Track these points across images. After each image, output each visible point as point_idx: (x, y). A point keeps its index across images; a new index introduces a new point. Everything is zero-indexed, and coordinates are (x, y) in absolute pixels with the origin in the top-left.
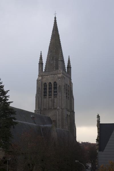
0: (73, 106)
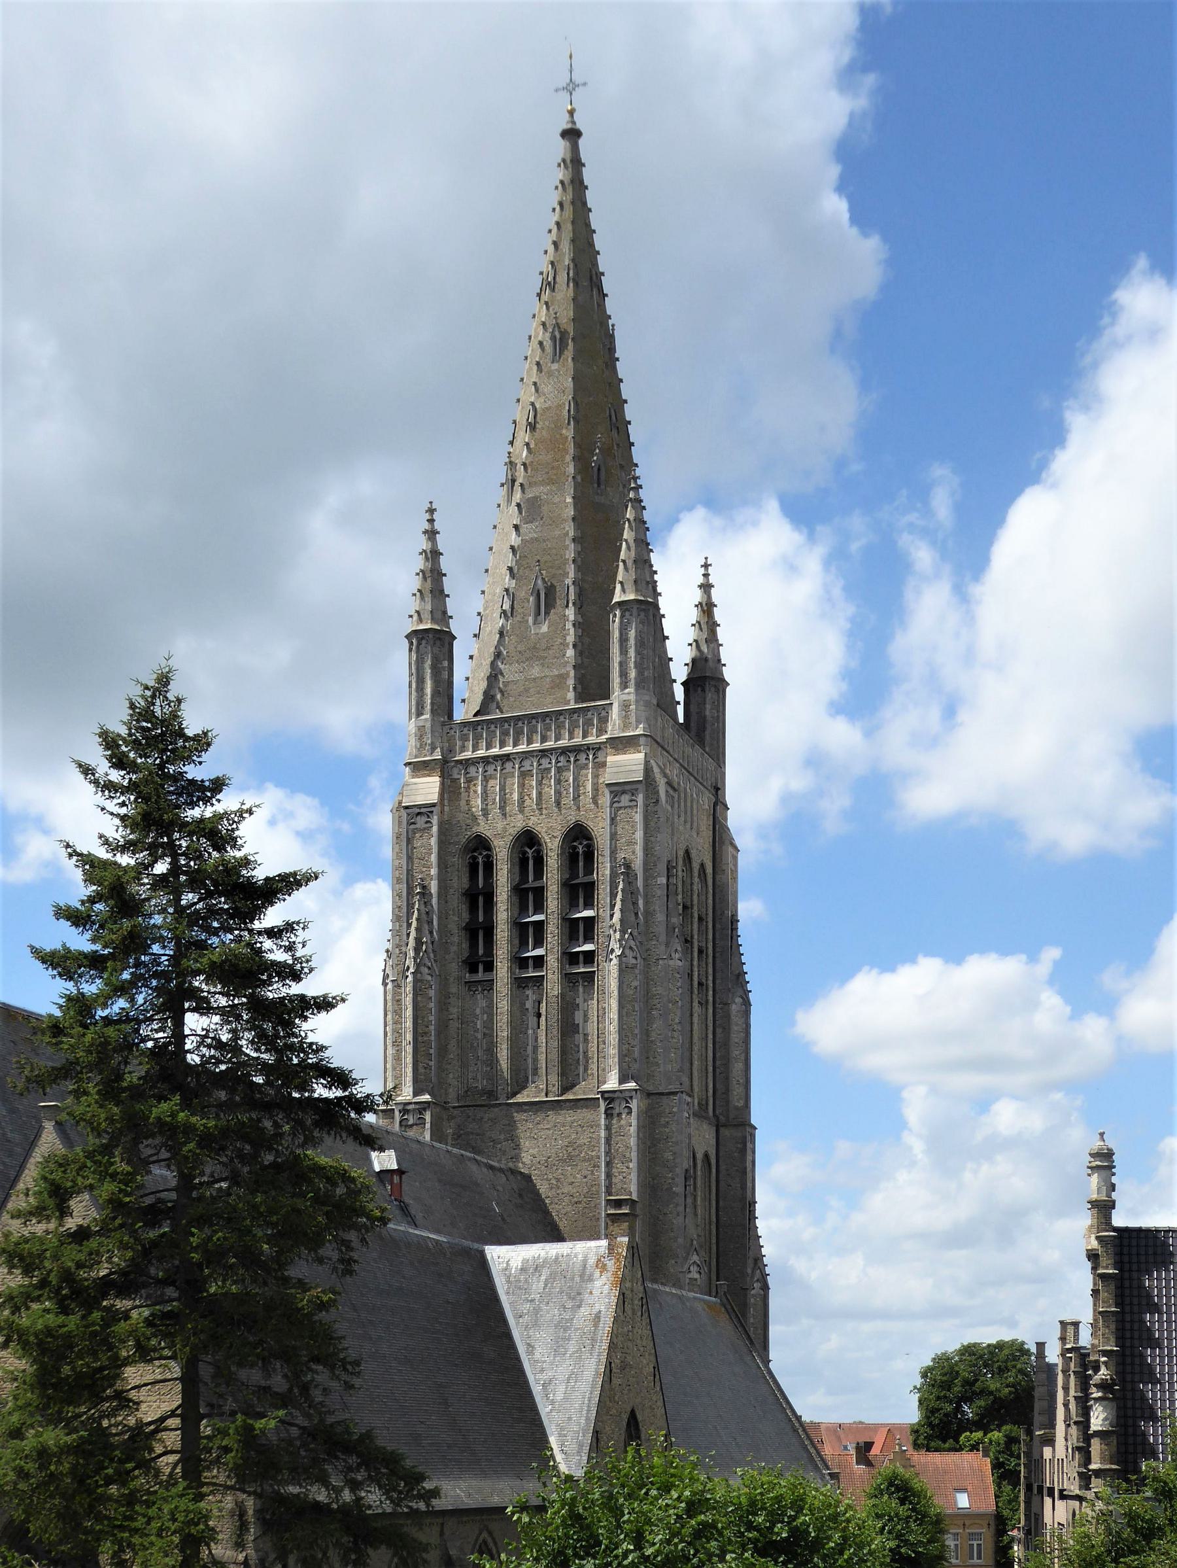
0: (738, 1067)
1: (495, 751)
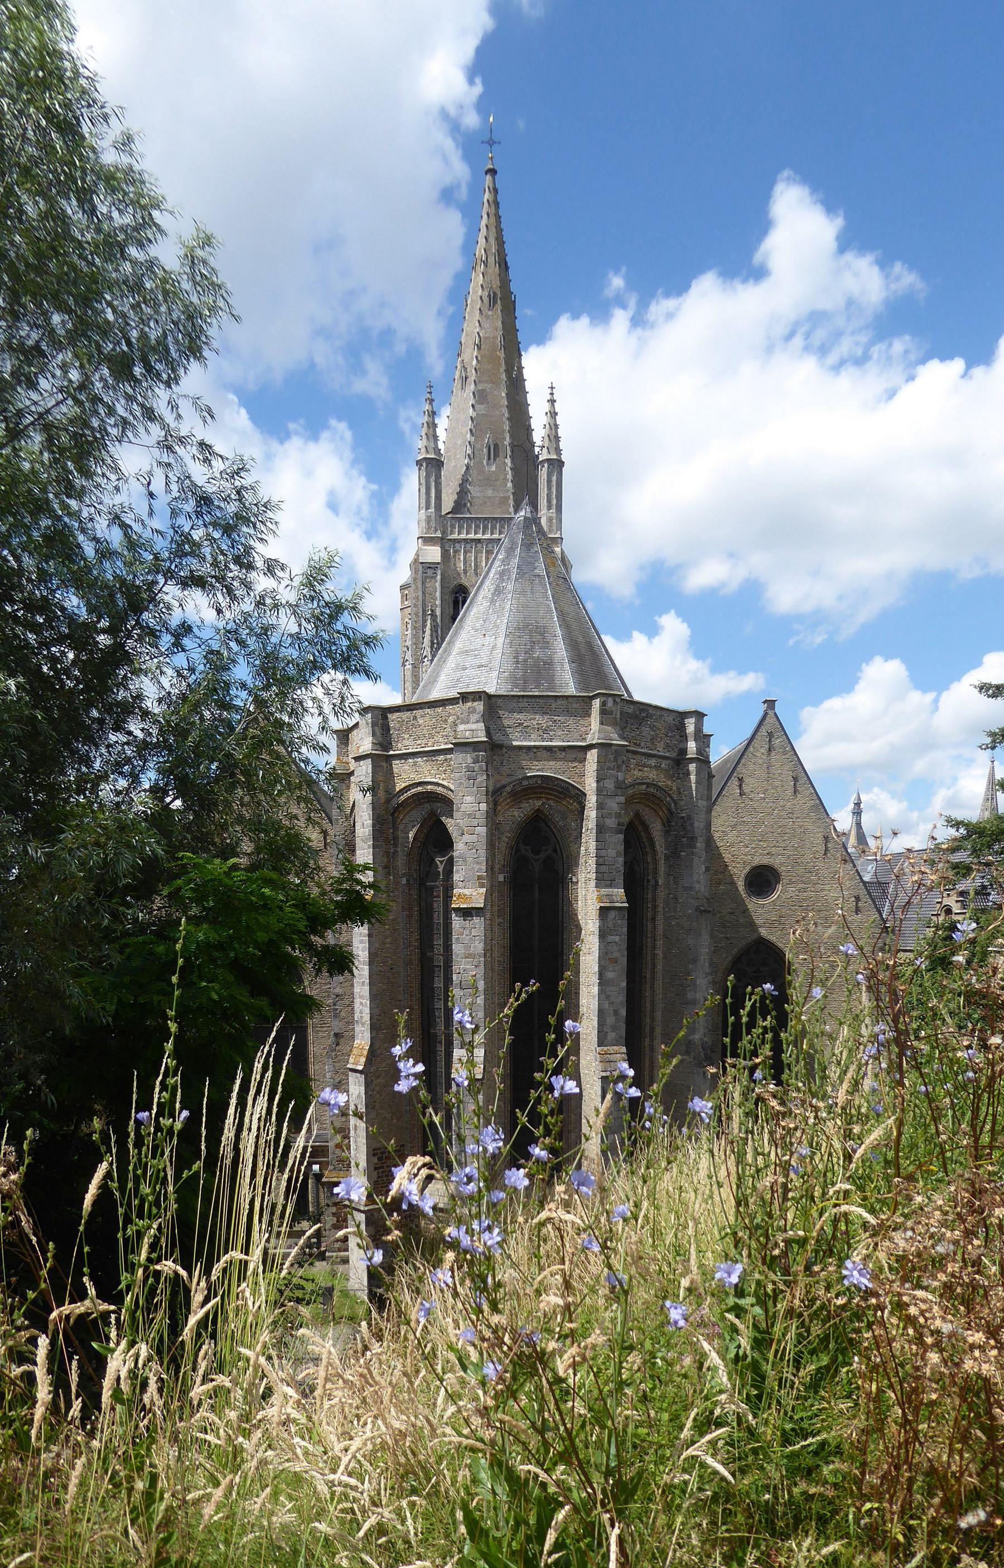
1: (472, 536)
